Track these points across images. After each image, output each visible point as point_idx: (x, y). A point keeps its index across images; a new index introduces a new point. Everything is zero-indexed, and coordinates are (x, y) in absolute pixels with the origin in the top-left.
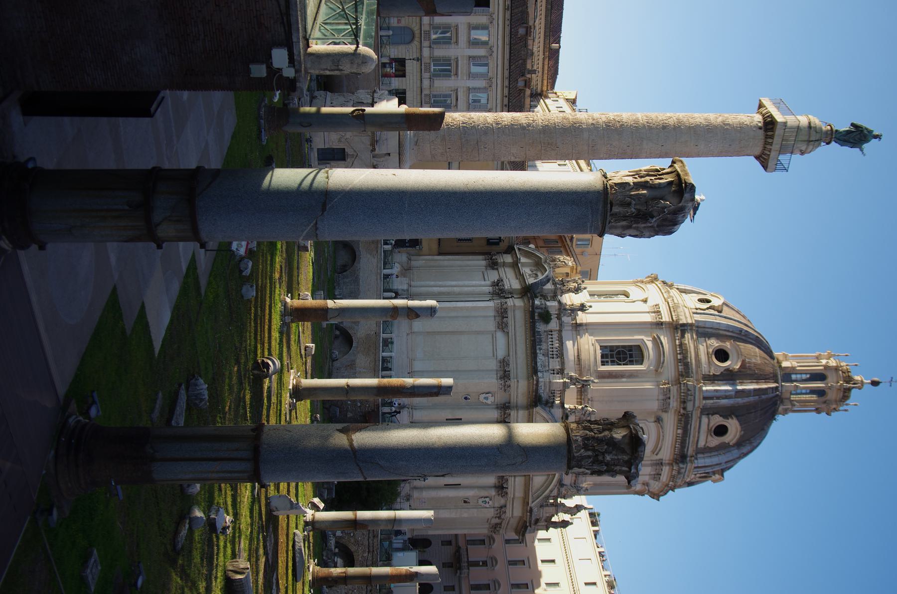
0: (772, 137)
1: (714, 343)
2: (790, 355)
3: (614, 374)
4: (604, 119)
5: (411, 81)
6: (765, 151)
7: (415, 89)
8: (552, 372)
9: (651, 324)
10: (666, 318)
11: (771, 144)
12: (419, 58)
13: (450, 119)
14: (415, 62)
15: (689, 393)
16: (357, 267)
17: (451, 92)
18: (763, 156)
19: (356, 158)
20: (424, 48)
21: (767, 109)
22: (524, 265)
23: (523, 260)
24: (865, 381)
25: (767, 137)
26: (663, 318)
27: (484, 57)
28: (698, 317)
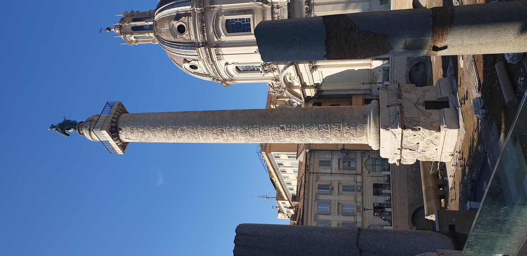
0: (112, 122)
1: (185, 36)
2: (151, 42)
3: (243, 13)
4: (225, 135)
5: (369, 200)
6: (119, 114)
7: (367, 195)
8: (279, 7)
9: (221, 47)
10: (213, 50)
11: (113, 118)
12: (364, 210)
13: (338, 136)
14: (367, 208)
15: (199, 3)
16: (409, 68)
17: (343, 192)
18: (121, 112)
19: (416, 103)
20: (361, 222)
21: (117, 144)
22: (297, 87)
23: (298, 91)
24: (113, 30)
25: (116, 123)
26: (214, 50)
27: (320, 214)
28: (195, 52)
